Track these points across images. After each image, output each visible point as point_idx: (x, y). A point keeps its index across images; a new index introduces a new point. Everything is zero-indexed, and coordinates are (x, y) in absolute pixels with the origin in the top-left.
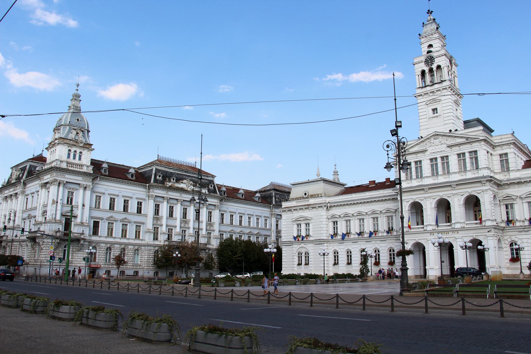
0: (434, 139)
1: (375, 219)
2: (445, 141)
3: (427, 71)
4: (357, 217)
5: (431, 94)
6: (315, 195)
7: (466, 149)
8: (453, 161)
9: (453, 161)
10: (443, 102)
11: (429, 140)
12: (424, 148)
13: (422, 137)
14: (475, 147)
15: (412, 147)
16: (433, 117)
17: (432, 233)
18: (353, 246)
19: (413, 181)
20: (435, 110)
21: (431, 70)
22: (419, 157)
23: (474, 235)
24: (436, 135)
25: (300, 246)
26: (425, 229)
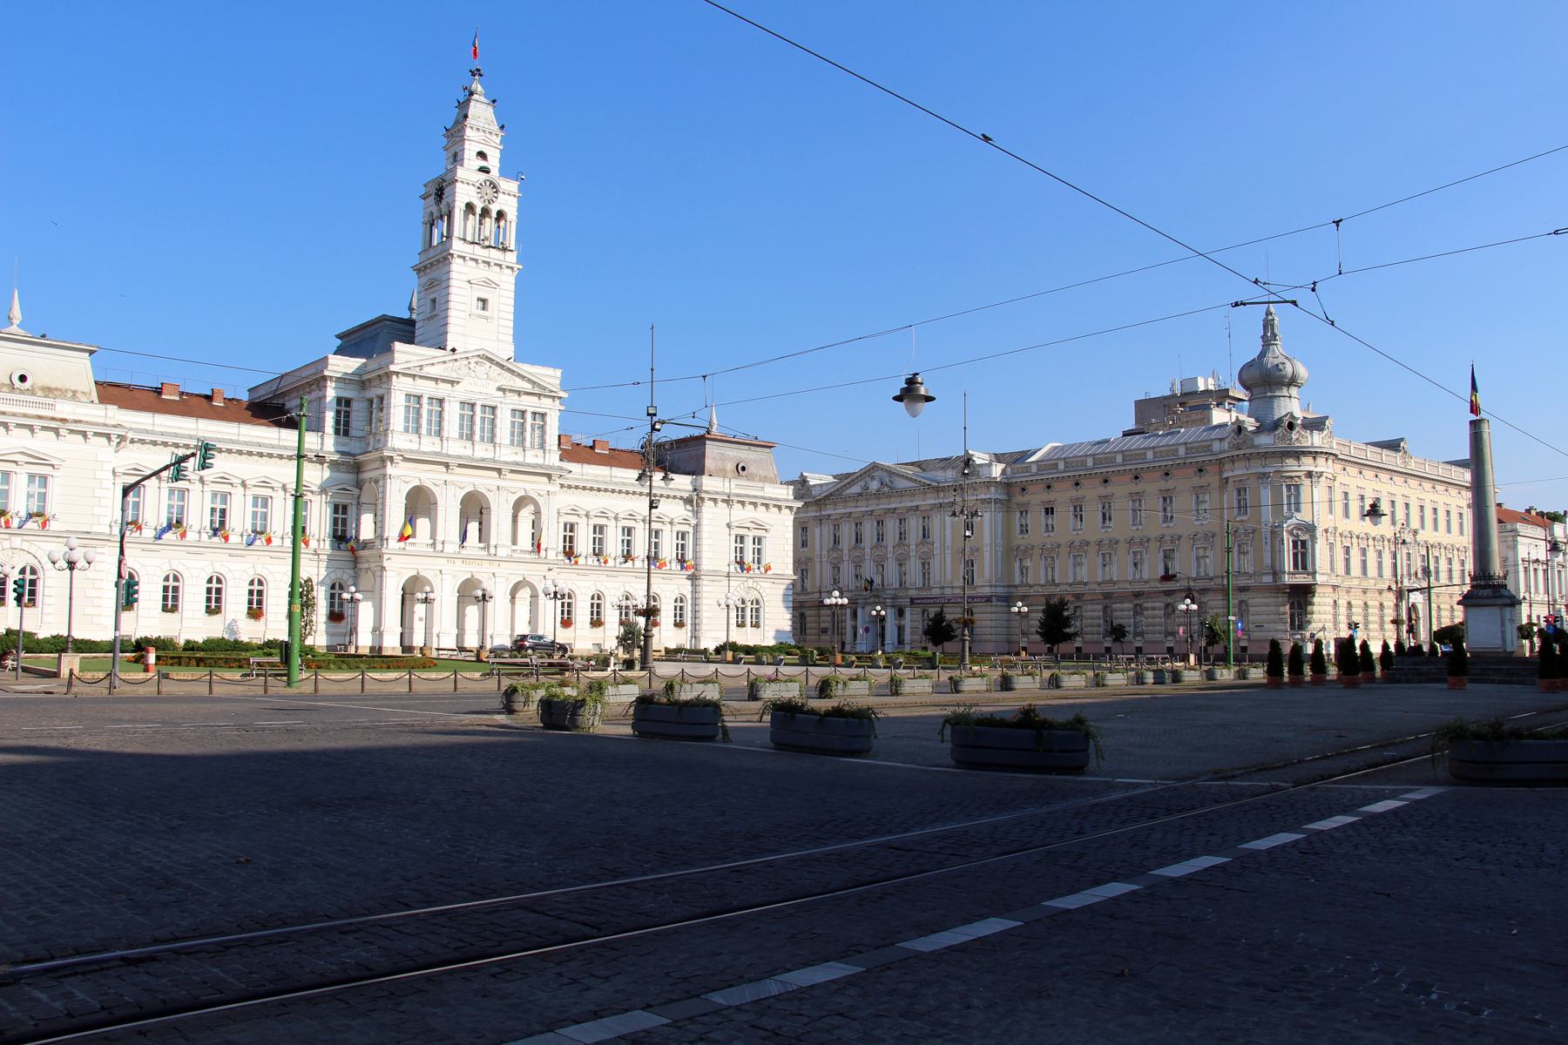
0: (476, 363)
2: (496, 375)
4: (123, 476)
5: (482, 266)
6: (61, 390)
7: (530, 404)
8: (504, 420)
9: (504, 420)
10: (502, 292)
11: (466, 362)
12: (454, 375)
14: (546, 405)
15: (433, 364)
16: (479, 316)
22: (442, 390)
23: (525, 573)
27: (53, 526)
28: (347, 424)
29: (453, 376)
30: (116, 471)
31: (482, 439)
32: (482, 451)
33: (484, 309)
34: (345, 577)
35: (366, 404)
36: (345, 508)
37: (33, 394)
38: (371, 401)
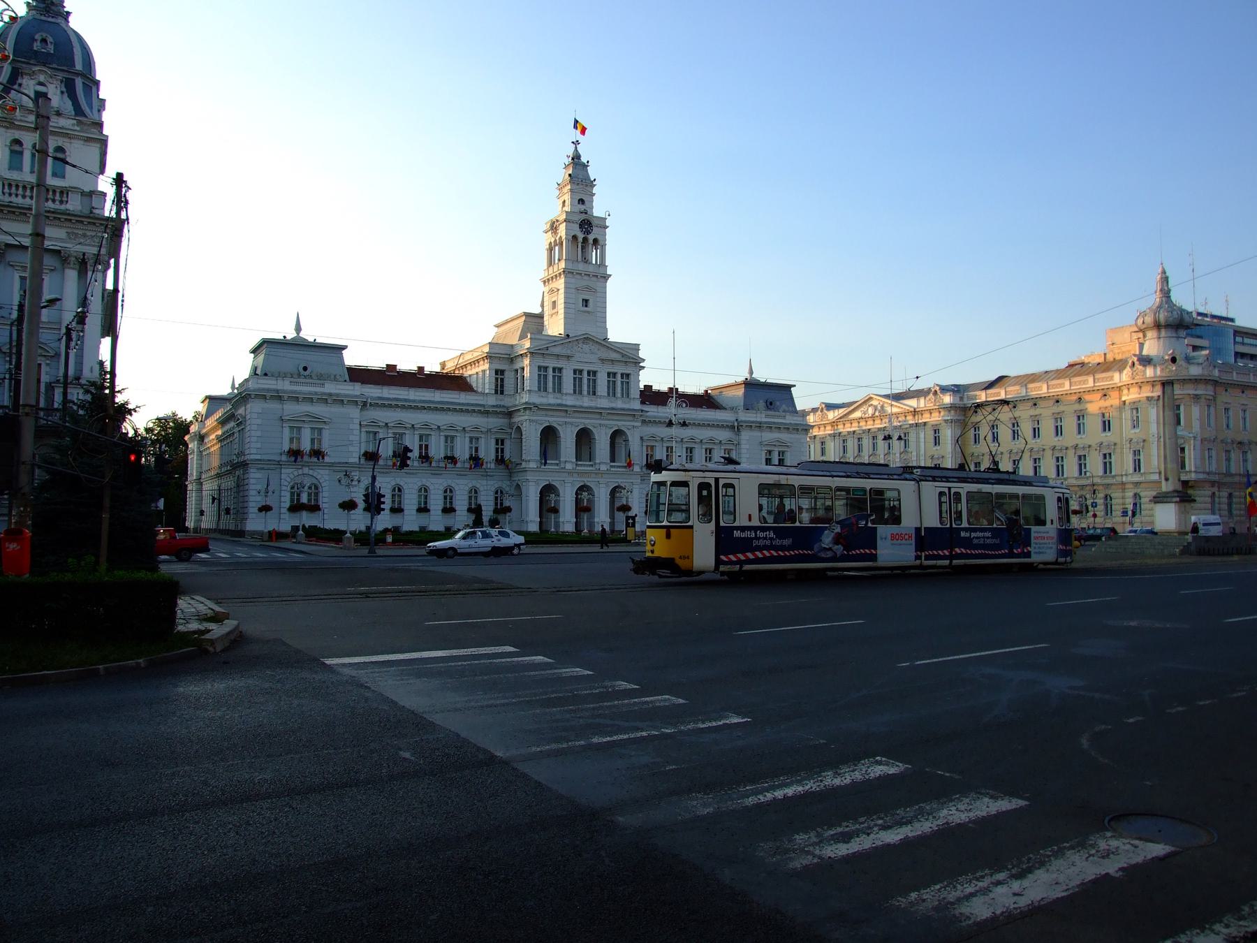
1: (450, 439)
3: (580, 240)
13: (568, 335)
17: (570, 473)
18: (434, 480)
19: (551, 396)
20: (586, 302)
21: (585, 240)
24: (587, 339)
25: (300, 472)
26: (562, 466)
27: (327, 459)
28: (502, 386)
29: (569, 352)
30: (362, 423)
31: (589, 393)
32: (586, 401)
33: (586, 306)
34: (504, 486)
35: (513, 373)
36: (503, 441)
37: (311, 377)
38: (517, 370)
